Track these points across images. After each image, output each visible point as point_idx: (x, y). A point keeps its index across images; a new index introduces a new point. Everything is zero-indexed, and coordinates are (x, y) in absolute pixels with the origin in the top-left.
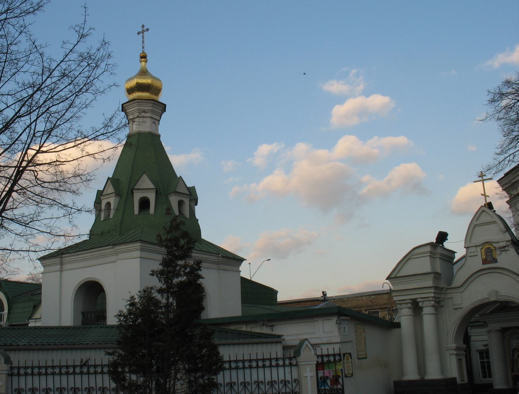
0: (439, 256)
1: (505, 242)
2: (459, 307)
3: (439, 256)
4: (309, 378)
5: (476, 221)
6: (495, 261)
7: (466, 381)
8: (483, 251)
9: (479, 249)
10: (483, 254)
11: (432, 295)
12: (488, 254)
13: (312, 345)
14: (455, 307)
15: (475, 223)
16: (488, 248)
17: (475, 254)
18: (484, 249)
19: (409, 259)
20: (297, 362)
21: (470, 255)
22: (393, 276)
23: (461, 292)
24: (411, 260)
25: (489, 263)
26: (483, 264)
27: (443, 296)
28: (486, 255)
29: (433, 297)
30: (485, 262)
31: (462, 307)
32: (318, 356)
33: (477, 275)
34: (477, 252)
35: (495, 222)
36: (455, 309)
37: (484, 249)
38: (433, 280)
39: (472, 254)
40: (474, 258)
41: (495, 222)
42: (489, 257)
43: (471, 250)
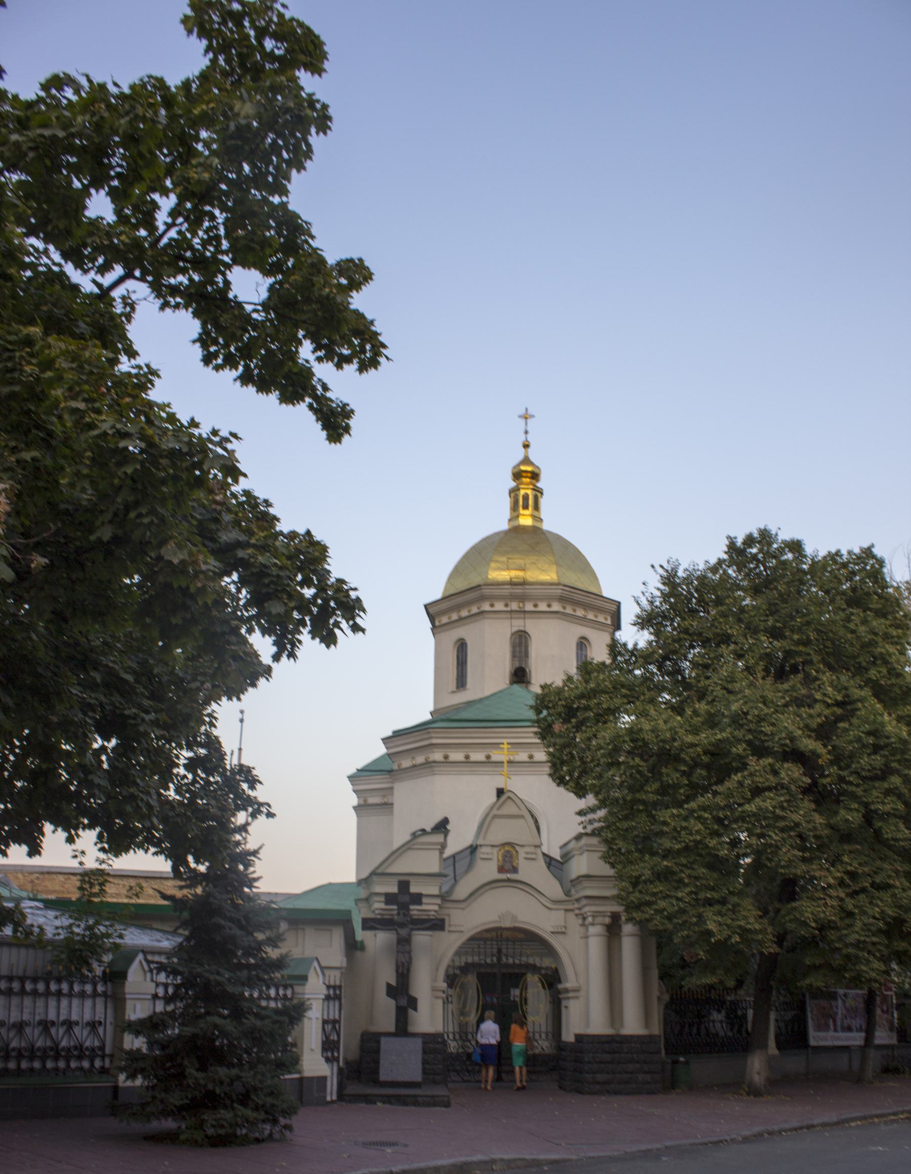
4: (314, 1020)
6: (515, 870)
8: (500, 853)
9: (495, 850)
10: (500, 858)
11: (436, 908)
13: (322, 968)
15: (495, 812)
16: (508, 852)
17: (490, 856)
19: (409, 848)
20: (293, 993)
21: (482, 856)
22: (380, 871)
24: (411, 853)
25: (507, 871)
29: (435, 911)
30: (501, 870)
31: (462, 929)
32: (329, 987)
35: (522, 817)
39: (486, 856)
41: (522, 817)
42: (508, 865)
43: (484, 850)
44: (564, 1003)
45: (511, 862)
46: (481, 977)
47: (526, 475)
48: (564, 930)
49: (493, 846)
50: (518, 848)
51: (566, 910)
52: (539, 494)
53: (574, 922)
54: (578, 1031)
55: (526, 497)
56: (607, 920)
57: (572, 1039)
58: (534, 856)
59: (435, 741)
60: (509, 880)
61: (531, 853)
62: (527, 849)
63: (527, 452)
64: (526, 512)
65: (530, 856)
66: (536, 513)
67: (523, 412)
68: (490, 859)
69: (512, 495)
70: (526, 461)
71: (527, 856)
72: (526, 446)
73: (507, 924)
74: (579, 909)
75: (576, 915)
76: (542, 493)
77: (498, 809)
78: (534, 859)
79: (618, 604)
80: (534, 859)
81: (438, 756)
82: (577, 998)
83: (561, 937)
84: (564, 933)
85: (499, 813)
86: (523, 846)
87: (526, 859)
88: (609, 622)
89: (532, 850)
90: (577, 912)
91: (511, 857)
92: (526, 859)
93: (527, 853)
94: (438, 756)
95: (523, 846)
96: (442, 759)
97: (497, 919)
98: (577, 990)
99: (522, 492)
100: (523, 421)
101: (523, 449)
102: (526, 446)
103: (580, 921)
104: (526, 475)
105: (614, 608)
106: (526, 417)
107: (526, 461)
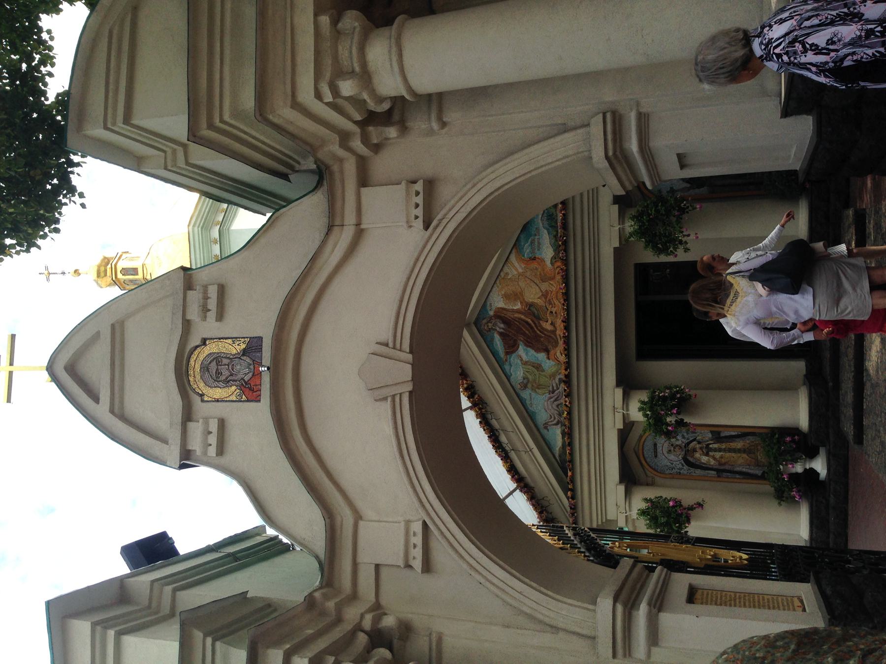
0: (168, 589)
1: (190, 293)
2: (418, 540)
3: (168, 589)
5: (96, 400)
7: (805, 590)
9: (201, 409)
12: (226, 373)
14: (417, 564)
15: (102, 409)
16: (205, 368)
17: (214, 426)
18: (201, 387)
23: (358, 517)
25: (257, 375)
26: (257, 400)
27: (352, 614)
28: (227, 382)
30: (250, 391)
31: (417, 527)
33: (297, 433)
34: (206, 420)
36: (427, 566)
37: (201, 387)
38: (229, 644)
39: (213, 439)
40: (234, 436)
43: (195, 445)
44: (672, 171)
45: (232, 358)
46: (642, 355)
48: (419, 186)
49: (188, 416)
50: (195, 341)
51: (364, 181)
53: (407, 152)
54: (773, 107)
55: (125, 271)
56: (352, 20)
57: (803, 127)
58: (213, 292)
60: (276, 369)
61: (206, 298)
62: (193, 314)
65: (212, 304)
68: (222, 424)
71: (212, 315)
73: (402, 372)
74: (344, 138)
75: (377, 148)
77: (96, 400)
78: (222, 290)
80: (222, 290)
82: (643, 119)
83: (445, 192)
84: (430, 185)
85: (105, 395)
86: (187, 325)
87: (220, 317)
89: (194, 296)
90: (357, 144)
91: (217, 358)
92: (220, 317)
93: (205, 310)
95: (187, 325)
97: (388, 405)
98: (615, 122)
99: (120, 276)
103: (392, 132)
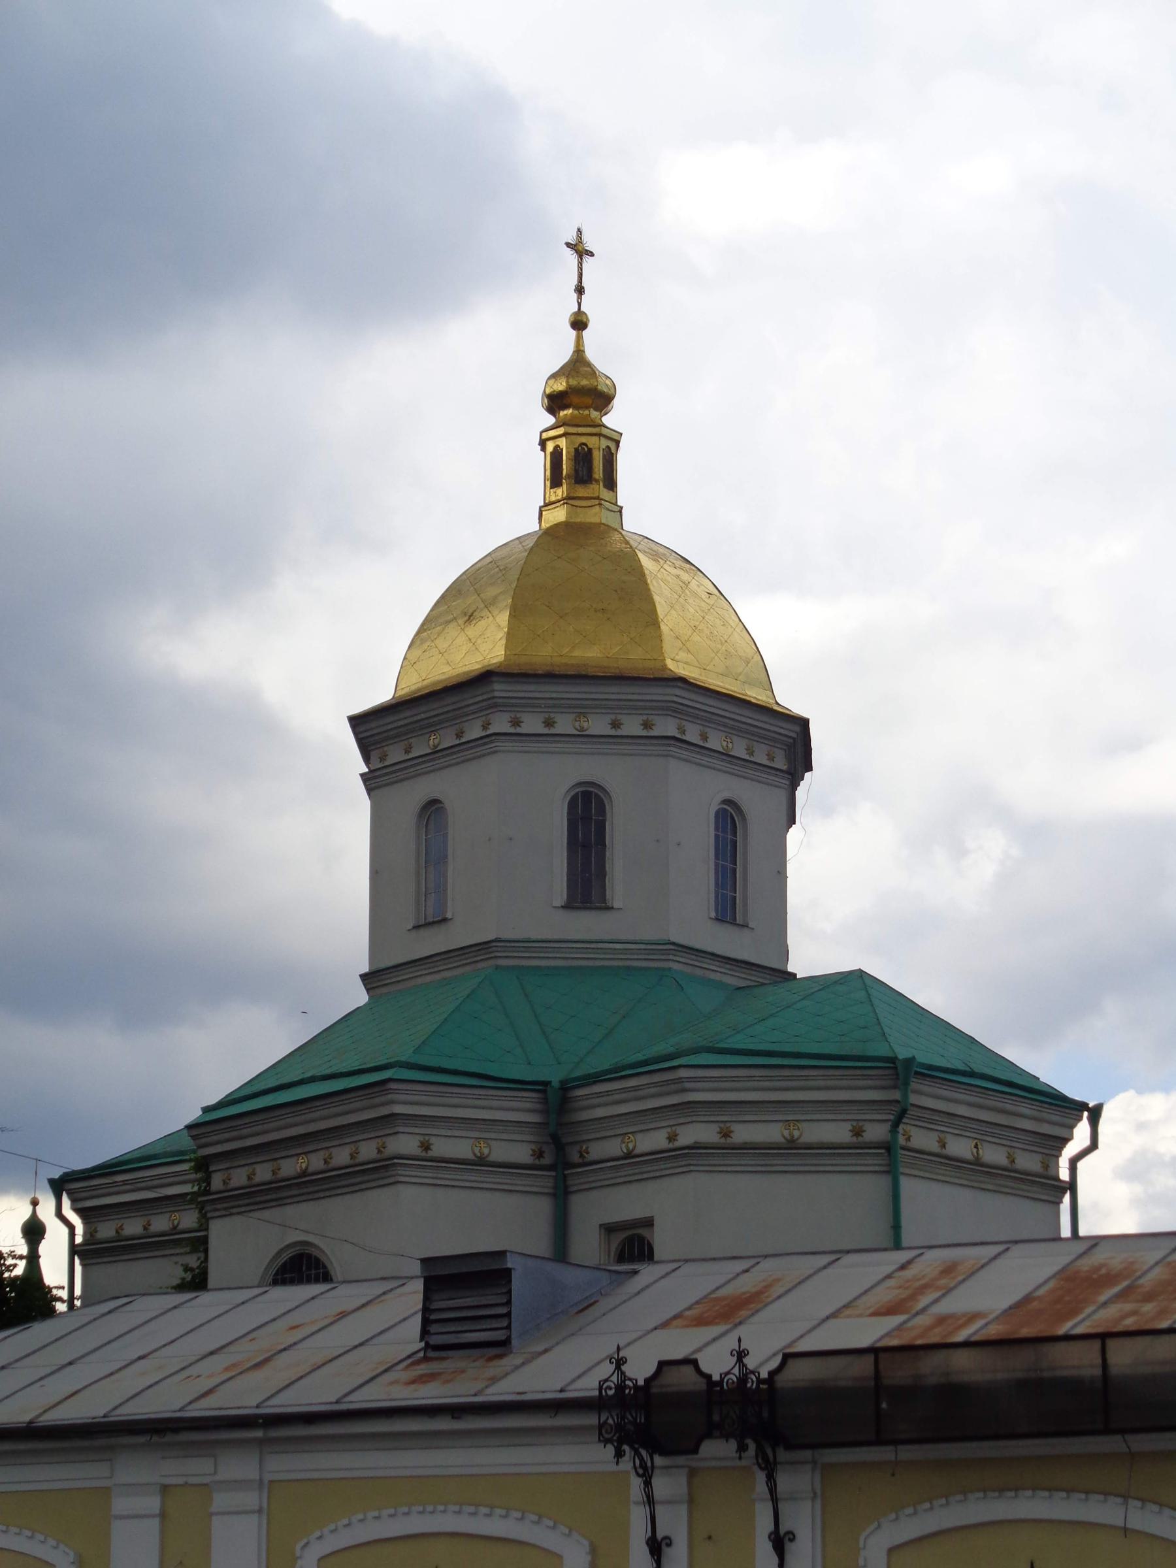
47: (579, 397)
52: (612, 446)
59: (398, 1109)
63: (579, 341)
64: (581, 491)
66: (605, 494)
67: (571, 237)
69: (550, 446)
70: (578, 363)
72: (579, 323)
76: (618, 443)
79: (804, 723)
81: (405, 1143)
88: (781, 763)
94: (405, 1143)
96: (418, 1152)
100: (571, 257)
101: (574, 333)
102: (579, 323)
104: (579, 397)
105: (793, 730)
106: (580, 250)
107: (578, 363)
